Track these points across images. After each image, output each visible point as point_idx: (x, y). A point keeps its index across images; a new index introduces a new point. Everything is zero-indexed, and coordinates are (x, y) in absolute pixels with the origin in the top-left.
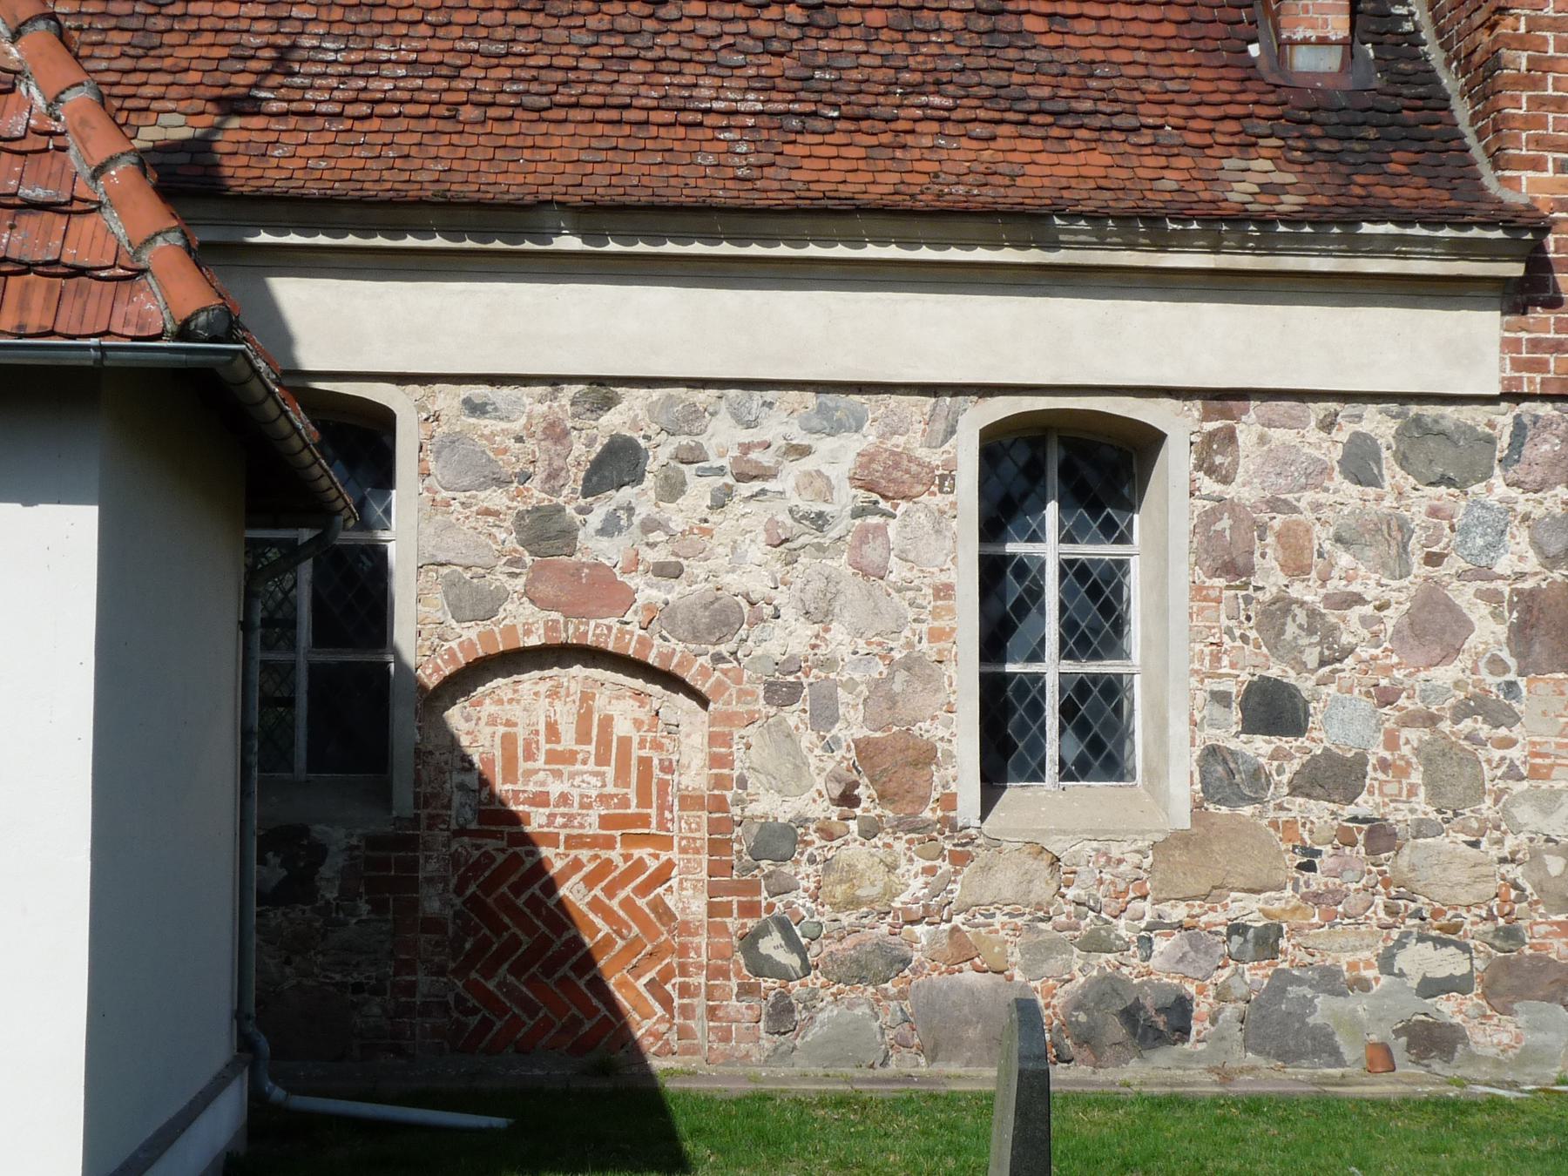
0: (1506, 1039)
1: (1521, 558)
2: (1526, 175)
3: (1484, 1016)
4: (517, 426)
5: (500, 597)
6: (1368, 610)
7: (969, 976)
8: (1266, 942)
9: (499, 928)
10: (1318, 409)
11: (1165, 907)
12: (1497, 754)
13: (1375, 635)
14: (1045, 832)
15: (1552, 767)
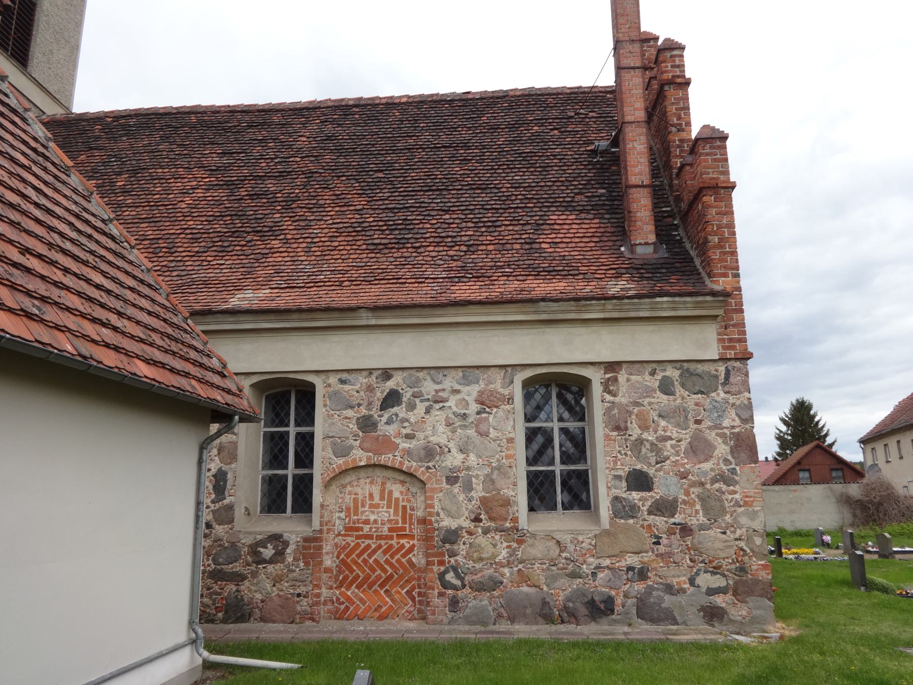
0: (744, 613)
1: (733, 420)
2: (722, 279)
3: (734, 603)
4: (357, 387)
5: (351, 448)
6: (673, 442)
7: (525, 589)
8: (642, 574)
9: (352, 571)
10: (649, 368)
11: (601, 561)
12: (730, 497)
13: (677, 452)
14: (552, 531)
15: (753, 501)
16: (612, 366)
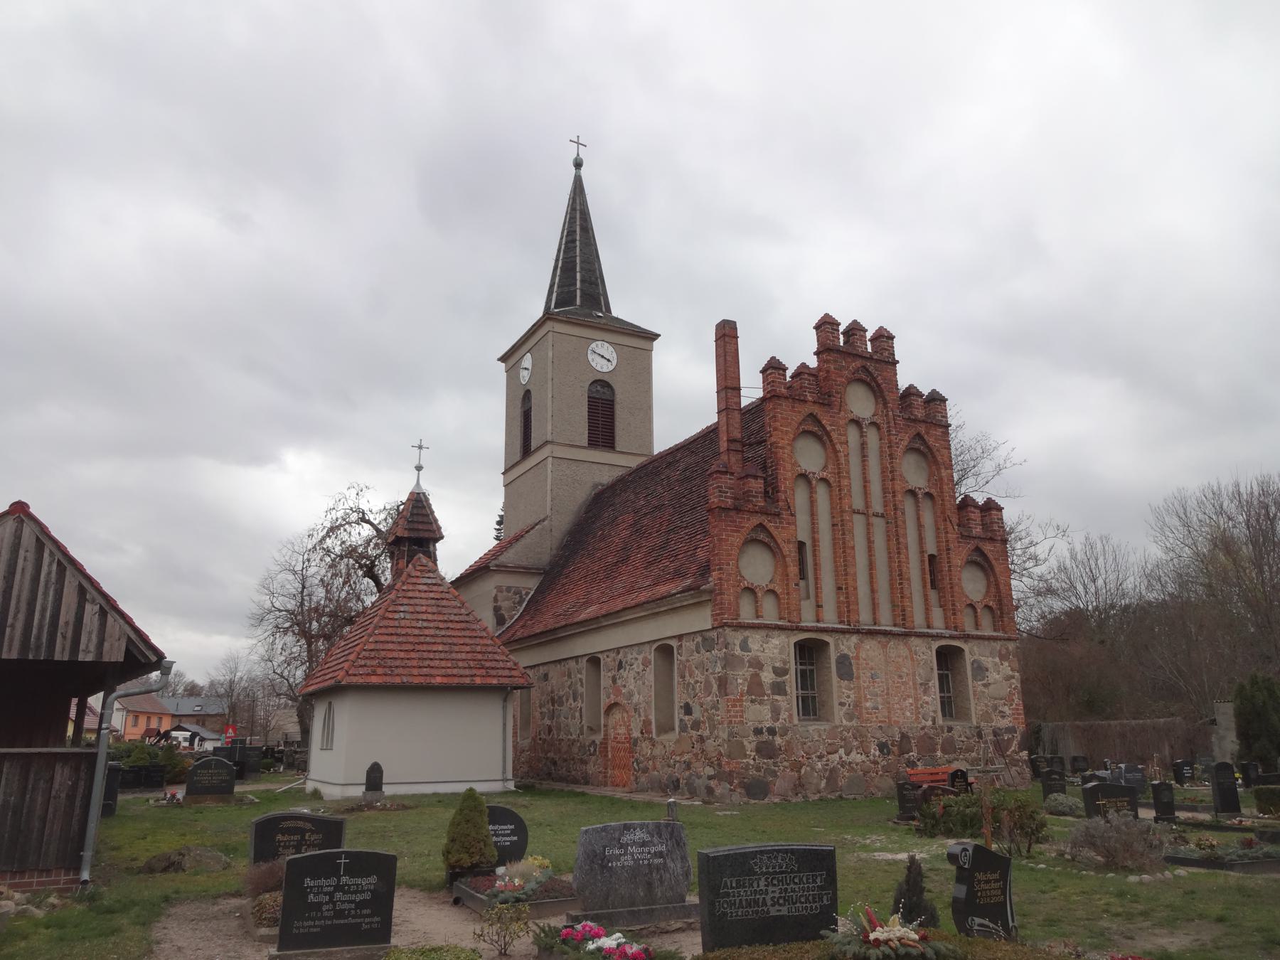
7: (656, 773)
8: (688, 765)
16: (680, 637)
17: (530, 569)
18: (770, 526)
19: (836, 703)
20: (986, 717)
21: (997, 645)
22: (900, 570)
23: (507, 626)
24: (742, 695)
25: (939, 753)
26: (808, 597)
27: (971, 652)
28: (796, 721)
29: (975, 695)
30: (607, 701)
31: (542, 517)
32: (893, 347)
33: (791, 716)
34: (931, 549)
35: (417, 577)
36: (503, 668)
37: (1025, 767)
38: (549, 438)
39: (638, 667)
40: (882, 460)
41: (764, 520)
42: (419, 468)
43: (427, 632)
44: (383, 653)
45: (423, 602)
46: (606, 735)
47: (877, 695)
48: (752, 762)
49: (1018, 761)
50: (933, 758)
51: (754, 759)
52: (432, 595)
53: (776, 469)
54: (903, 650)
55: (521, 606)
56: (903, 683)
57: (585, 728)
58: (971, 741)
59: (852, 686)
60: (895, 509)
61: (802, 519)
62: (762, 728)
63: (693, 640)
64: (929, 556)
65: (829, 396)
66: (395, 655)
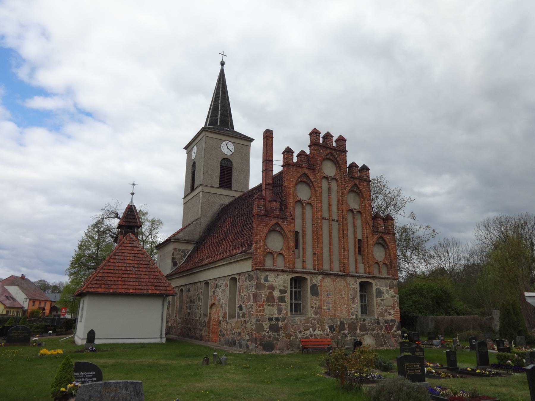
7: (227, 337)
8: (240, 334)
16: (239, 274)
17: (190, 241)
18: (282, 224)
19: (309, 306)
20: (382, 314)
21: (388, 282)
22: (343, 246)
23: (178, 266)
24: (263, 302)
25: (358, 331)
26: (299, 257)
27: (376, 284)
28: (289, 315)
29: (377, 304)
30: (211, 302)
31: (197, 218)
32: (345, 145)
33: (287, 312)
34: (359, 236)
35: (127, 243)
36: (163, 286)
37: (399, 338)
38: (201, 183)
39: (223, 287)
40: (338, 195)
41: (279, 221)
42: (133, 194)
43: (128, 269)
44: (106, 278)
45: (128, 255)
46: (210, 318)
47: (329, 303)
48: (267, 334)
49: (396, 335)
50: (355, 333)
51: (268, 332)
52: (133, 252)
53: (286, 198)
54: (343, 283)
55: (185, 258)
56: (342, 298)
57: (202, 314)
58: (374, 326)
59: (318, 299)
60: (343, 218)
61: (298, 222)
62: (273, 318)
63: (245, 276)
64: (358, 240)
65: (314, 166)
66: (111, 279)
